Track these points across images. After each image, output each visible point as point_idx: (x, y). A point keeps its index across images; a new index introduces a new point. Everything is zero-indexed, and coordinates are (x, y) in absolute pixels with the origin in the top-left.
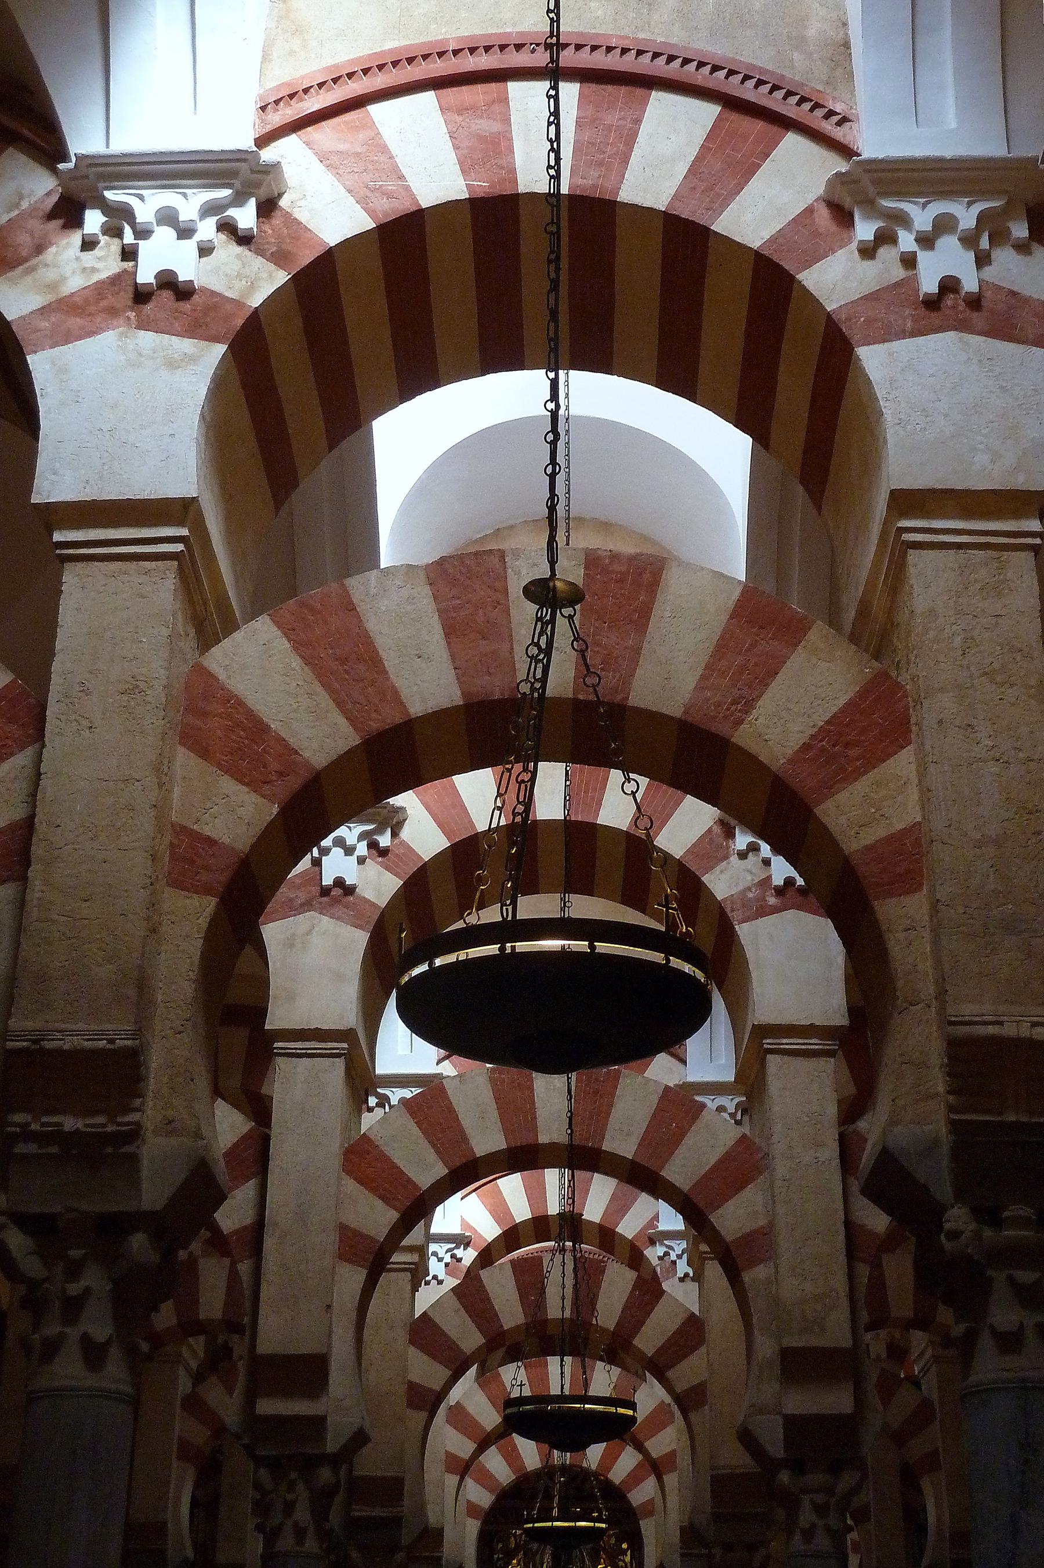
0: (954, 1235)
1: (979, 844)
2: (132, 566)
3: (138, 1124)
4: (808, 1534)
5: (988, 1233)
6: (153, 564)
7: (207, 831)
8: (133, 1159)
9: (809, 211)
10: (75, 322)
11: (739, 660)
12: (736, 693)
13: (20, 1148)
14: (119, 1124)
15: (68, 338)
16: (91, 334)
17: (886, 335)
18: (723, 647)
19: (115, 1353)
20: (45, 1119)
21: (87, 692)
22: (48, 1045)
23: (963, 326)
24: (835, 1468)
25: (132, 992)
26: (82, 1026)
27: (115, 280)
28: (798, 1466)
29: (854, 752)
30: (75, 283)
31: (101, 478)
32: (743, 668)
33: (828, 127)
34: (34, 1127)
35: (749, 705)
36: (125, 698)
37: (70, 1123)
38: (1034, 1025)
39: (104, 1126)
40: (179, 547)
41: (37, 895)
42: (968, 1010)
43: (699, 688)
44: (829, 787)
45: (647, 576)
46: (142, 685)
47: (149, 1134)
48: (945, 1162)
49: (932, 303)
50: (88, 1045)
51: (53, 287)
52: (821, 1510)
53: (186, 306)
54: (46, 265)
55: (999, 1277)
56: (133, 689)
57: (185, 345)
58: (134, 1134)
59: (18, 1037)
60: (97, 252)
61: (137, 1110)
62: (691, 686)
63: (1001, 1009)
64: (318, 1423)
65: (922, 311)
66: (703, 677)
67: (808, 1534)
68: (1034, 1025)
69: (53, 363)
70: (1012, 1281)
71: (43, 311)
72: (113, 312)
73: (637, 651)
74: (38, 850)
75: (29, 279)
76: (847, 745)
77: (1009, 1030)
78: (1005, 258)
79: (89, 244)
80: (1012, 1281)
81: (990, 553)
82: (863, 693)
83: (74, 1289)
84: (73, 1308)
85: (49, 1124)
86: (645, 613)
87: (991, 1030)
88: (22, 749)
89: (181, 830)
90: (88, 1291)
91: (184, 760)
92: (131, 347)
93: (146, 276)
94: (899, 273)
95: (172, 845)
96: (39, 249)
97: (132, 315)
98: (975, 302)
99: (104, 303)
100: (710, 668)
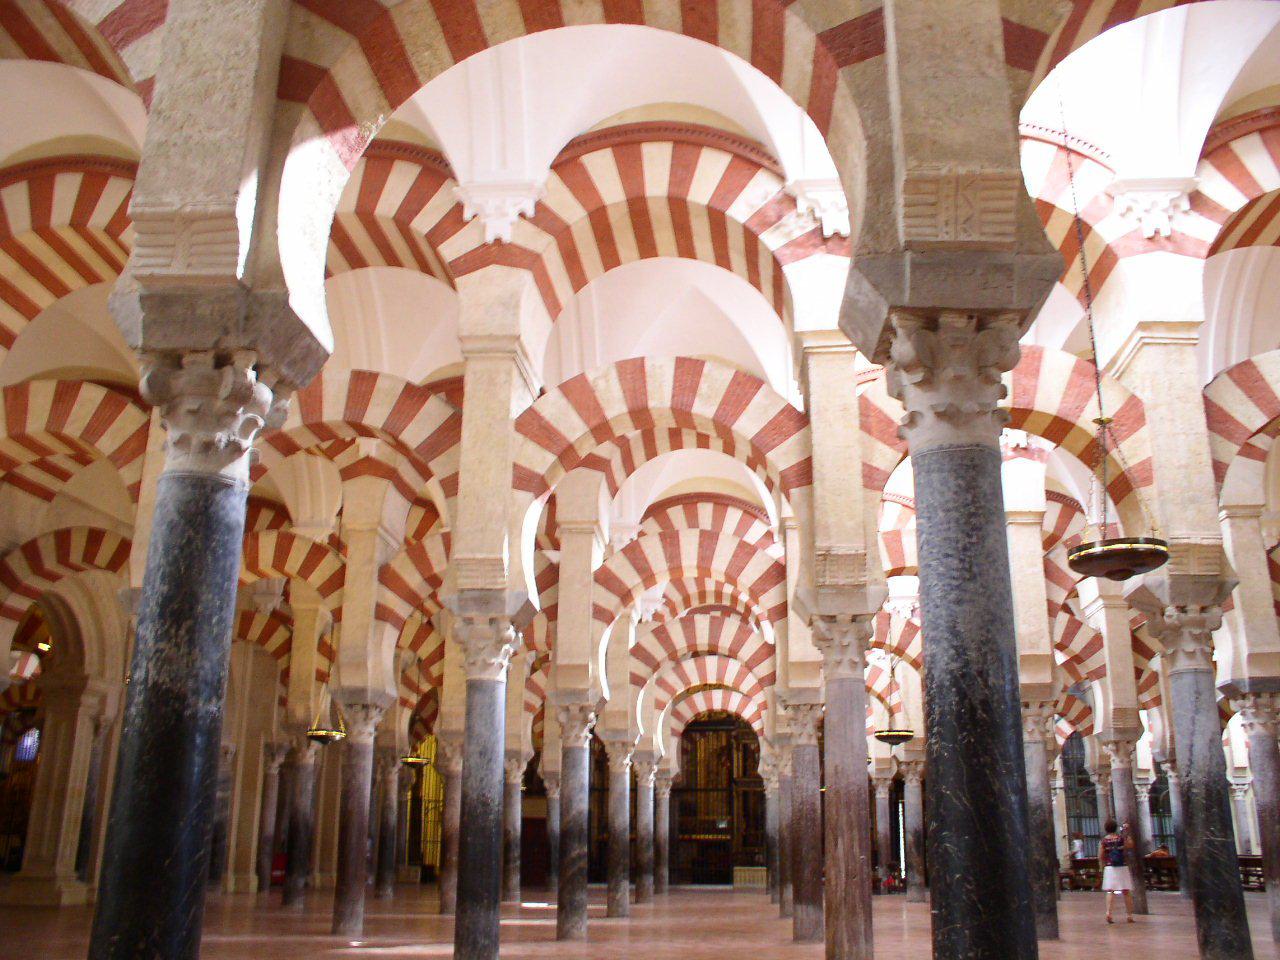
0: (1170, 616)
1: (1179, 468)
2: (837, 356)
4: (1031, 733)
5: (1183, 615)
6: (844, 356)
7: (875, 464)
8: (864, 595)
9: (1096, 198)
10: (800, 251)
11: (1076, 390)
12: (1077, 404)
13: (822, 591)
17: (1133, 253)
18: (1070, 385)
22: (833, 553)
23: (1163, 248)
24: (1041, 706)
25: (861, 531)
27: (814, 232)
29: (1124, 428)
30: (797, 234)
32: (1078, 395)
33: (1102, 159)
34: (827, 583)
35: (1082, 410)
38: (1203, 538)
43: (1062, 403)
45: (1037, 355)
49: (1150, 239)
51: (790, 233)
52: (1036, 723)
53: (846, 244)
54: (784, 225)
55: (1186, 631)
58: (864, 585)
60: (804, 219)
63: (1190, 532)
65: (1146, 242)
66: (1064, 398)
67: (1031, 733)
68: (1203, 538)
70: (1190, 633)
71: (787, 246)
72: (815, 246)
73: (1035, 387)
75: (778, 232)
76: (1122, 425)
77: (1193, 541)
78: (1179, 217)
79: (799, 216)
80: (1190, 633)
81: (1179, 347)
82: (1127, 404)
86: (1038, 371)
87: (1186, 541)
93: (828, 232)
94: (1135, 225)
96: (780, 218)
98: (1168, 238)
99: (811, 243)
100: (1066, 394)
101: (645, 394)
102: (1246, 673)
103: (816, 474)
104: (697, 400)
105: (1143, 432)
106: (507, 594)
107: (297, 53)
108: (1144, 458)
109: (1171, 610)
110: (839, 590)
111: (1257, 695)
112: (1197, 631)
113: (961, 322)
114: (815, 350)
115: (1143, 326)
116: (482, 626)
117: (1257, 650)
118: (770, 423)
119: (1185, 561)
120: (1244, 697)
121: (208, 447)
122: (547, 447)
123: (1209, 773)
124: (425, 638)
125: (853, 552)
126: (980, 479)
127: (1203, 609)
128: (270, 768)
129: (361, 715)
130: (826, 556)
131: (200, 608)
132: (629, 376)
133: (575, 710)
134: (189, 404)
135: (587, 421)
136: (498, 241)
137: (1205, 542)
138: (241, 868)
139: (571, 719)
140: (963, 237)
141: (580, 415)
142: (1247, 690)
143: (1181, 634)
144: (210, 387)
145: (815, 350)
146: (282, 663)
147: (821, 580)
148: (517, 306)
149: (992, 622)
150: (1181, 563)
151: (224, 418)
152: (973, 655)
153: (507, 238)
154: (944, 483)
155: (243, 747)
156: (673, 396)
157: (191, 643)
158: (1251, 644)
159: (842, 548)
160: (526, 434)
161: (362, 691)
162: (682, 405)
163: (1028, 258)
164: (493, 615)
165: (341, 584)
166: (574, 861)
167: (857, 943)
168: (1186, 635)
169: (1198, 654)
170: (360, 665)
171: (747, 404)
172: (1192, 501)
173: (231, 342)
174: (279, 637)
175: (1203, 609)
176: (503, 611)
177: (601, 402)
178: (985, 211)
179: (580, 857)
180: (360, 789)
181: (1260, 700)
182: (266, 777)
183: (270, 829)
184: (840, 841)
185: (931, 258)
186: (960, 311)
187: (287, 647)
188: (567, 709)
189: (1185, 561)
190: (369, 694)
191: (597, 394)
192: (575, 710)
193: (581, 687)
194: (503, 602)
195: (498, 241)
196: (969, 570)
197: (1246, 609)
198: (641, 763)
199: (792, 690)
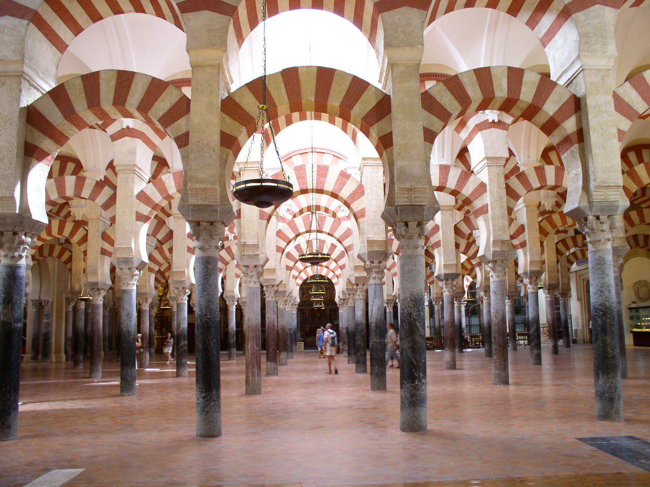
1: (373, 212)
13: (243, 257)
28: (357, 285)
35: (341, 190)
37: (250, 253)
40: (258, 168)
42: (369, 236)
44: (352, 202)
48: (367, 256)
55: (373, 270)
58: (258, 255)
62: (333, 186)
64: (274, 280)
73: (325, 181)
77: (375, 239)
86: (326, 175)
102: (443, 272)
103: (242, 216)
105: (363, 198)
106: (134, 259)
107: (29, 141)
108: (362, 208)
109: (368, 263)
110: (250, 256)
111: (447, 280)
112: (377, 270)
113: (206, 224)
115: (364, 159)
116: (126, 270)
117: (447, 263)
119: (373, 246)
120: (443, 280)
121: (13, 257)
122: (148, 205)
123: (377, 319)
126: (209, 265)
127: (380, 262)
128: (68, 308)
129: (97, 293)
130: (244, 245)
131: (14, 300)
133: (181, 288)
134: (7, 246)
136: (128, 127)
137: (379, 239)
138: (58, 352)
139: (179, 292)
140: (204, 203)
142: (443, 278)
143: (371, 271)
144: (12, 241)
146: (68, 266)
148: (135, 153)
149: (209, 302)
150: (372, 247)
151: (17, 249)
152: (204, 310)
153: (131, 126)
154: (200, 266)
155: (55, 300)
157: (12, 310)
158: (445, 260)
159: (250, 242)
160: (140, 200)
161: (97, 283)
163: (223, 206)
164: (130, 267)
165: (86, 241)
166: (181, 347)
167: (255, 377)
168: (373, 272)
169: (377, 278)
170: (95, 273)
172: (376, 224)
173: (17, 229)
174: (66, 255)
175: (380, 262)
176: (133, 265)
177: (167, 188)
178: (210, 196)
179: (184, 345)
180: (98, 322)
181: (448, 282)
182: (67, 312)
183: (70, 334)
184: (249, 343)
185: (197, 208)
186: (205, 222)
187: (70, 260)
188: (178, 288)
189: (373, 246)
190: (100, 285)
192: (181, 288)
194: (133, 262)
195: (128, 127)
196: (204, 289)
197: (443, 247)
198: (229, 301)
199: (265, 279)
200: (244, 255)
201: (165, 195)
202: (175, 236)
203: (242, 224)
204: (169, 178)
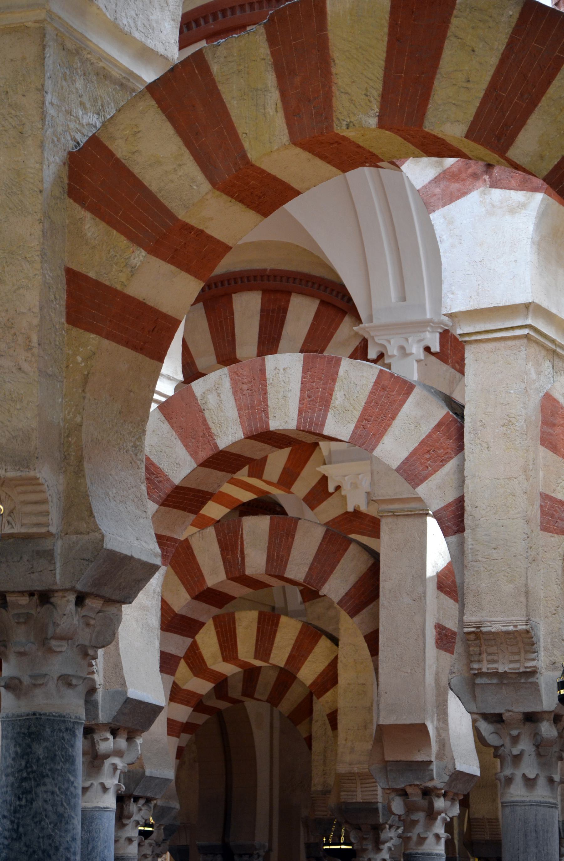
2: (501, 344)
3: (534, 667)
8: (536, 686)
13: (479, 681)
14: (526, 668)
15: (451, 198)
16: (464, 194)
19: (542, 781)
20: (490, 666)
21: (484, 426)
22: (484, 629)
25: (523, 599)
26: (499, 619)
31: (478, 294)
34: (484, 670)
36: (504, 428)
37: (502, 669)
39: (519, 669)
41: (470, 547)
46: (513, 420)
47: (543, 670)
50: (504, 629)
56: (508, 423)
57: (518, 196)
58: (533, 673)
59: (469, 626)
61: (534, 660)
69: (445, 218)
71: (436, 180)
74: (468, 521)
83: (515, 752)
84: (517, 759)
85: (492, 669)
88: (456, 455)
89: (545, 497)
90: (522, 752)
91: (543, 452)
92: (488, 201)
95: (541, 506)
97: (486, 177)
101: (266, 411)
104: (330, 416)
114: (474, 338)
118: (422, 443)
124: (305, 657)
125: (511, 628)
132: (245, 387)
135: (193, 454)
141: (186, 446)
145: (474, 338)
147: (476, 666)
156: (300, 412)
162: (311, 424)
171: (393, 418)
177: (211, 425)
191: (207, 415)
193: (420, 757)
200: (480, 674)
201: (204, 455)
202: (385, 585)
203: (469, 556)
204: (216, 388)
